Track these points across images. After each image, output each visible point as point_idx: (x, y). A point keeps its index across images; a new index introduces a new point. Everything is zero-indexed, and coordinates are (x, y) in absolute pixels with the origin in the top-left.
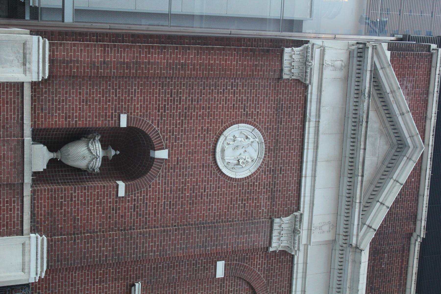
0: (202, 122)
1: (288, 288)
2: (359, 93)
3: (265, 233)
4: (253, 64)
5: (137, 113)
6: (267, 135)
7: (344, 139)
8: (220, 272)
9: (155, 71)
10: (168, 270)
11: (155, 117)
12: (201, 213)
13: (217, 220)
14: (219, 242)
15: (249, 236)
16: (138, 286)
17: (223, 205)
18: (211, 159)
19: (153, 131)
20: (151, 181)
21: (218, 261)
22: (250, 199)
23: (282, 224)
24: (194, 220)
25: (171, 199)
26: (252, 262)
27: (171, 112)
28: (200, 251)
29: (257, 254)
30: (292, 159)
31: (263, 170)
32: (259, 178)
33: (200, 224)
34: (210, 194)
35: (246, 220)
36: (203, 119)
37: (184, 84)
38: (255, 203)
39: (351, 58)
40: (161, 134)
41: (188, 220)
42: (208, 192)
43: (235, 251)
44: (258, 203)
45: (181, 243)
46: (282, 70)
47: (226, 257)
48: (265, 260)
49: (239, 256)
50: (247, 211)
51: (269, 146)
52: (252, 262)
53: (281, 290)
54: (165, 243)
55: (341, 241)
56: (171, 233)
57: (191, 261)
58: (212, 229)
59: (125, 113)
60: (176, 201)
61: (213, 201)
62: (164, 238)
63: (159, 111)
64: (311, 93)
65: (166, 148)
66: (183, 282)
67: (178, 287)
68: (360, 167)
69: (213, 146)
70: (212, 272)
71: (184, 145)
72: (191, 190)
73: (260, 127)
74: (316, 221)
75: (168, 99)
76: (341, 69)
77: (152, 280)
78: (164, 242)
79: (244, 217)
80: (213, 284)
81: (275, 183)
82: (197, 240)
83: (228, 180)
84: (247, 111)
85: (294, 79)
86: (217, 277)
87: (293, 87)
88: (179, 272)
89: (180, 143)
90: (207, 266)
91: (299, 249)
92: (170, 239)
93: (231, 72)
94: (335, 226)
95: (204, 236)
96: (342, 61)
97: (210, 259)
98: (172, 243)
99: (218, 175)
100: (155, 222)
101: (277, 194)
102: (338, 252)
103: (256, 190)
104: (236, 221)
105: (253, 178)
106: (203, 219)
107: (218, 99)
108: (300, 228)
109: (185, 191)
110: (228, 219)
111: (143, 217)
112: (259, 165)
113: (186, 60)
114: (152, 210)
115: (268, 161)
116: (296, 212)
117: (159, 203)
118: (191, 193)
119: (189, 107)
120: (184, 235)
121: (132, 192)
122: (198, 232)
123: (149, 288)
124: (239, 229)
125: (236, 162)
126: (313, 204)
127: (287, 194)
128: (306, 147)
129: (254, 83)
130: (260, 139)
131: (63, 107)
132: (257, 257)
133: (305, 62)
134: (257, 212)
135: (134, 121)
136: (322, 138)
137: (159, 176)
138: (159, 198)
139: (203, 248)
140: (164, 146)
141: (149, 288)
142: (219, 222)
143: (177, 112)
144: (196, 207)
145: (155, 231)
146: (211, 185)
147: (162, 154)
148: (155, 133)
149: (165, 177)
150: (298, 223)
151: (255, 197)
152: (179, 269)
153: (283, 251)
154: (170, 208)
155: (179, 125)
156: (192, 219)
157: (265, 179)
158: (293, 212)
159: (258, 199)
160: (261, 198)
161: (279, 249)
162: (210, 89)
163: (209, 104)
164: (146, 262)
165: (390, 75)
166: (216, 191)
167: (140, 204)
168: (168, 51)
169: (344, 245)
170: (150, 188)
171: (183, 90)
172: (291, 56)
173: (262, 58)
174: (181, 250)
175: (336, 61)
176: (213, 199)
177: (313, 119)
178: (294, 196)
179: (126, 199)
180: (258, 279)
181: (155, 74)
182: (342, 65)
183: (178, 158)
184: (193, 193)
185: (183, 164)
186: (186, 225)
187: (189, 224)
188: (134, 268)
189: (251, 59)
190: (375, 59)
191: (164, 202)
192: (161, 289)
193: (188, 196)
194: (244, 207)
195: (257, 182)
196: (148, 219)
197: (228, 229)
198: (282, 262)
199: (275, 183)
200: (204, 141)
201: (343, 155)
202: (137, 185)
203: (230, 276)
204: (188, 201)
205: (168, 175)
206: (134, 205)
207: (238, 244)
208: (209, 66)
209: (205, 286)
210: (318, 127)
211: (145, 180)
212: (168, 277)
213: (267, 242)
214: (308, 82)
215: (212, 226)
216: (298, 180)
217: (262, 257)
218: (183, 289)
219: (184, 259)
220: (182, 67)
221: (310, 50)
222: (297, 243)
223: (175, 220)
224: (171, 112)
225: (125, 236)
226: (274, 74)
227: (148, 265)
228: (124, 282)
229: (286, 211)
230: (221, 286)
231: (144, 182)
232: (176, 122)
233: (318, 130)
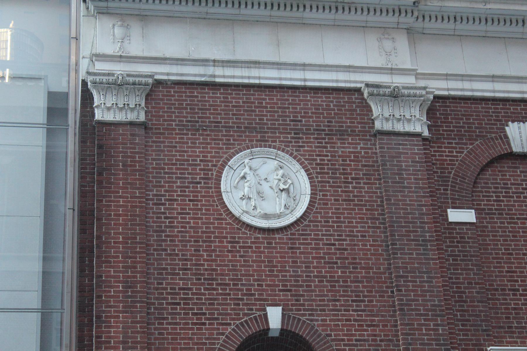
0: (220, 251)
1: (488, 104)
3: (400, 144)
4: (122, 170)
6: (238, 145)
7: (241, 18)
8: (467, 216)
9: (138, 332)
10: (465, 302)
11: (214, 329)
12: (370, 250)
13: (380, 223)
14: (416, 218)
15: (406, 170)
18: (280, 236)
19: (237, 333)
20: (320, 334)
21: (448, 219)
22: (343, 169)
23: (384, 117)
24: (382, 261)
25: (348, 301)
26: (448, 164)
27: (204, 304)
28: (431, 250)
29: (435, 156)
30: (277, 104)
31: (296, 151)
32: (309, 155)
33: (387, 251)
34: (338, 235)
35: (379, 175)
36: (214, 251)
37: (158, 284)
38: (350, 161)
39: (109, 11)
41: (382, 270)
42: (335, 240)
43: (431, 192)
44: (350, 157)
45: (420, 282)
46: (132, 124)
47: (440, 207)
48: (444, 143)
49: (439, 185)
50: (364, 174)
51: (257, 141)
52: (448, 164)
53: (492, 116)
54: (422, 308)
55: (409, 20)
56: (404, 298)
57: (450, 265)
58: (394, 231)
60: (352, 291)
61: (350, 231)
62: (412, 310)
63: (204, 324)
64: (168, 74)
65: (265, 310)
66: (484, 276)
67: (493, 285)
69: (259, 233)
71: (258, 280)
72: (333, 268)
73: (225, 156)
74: (378, 61)
75: (184, 309)
76: (128, 27)
77: (484, 328)
78: (420, 310)
79: (375, 179)
80: (487, 227)
81: (317, 130)
82: (415, 256)
83: (314, 206)
84: (200, 178)
85: (146, 103)
86: (475, 221)
87: (159, 104)
88: (469, 283)
89: (256, 287)
90: (457, 238)
91: (425, 88)
92: (413, 300)
93: (136, 207)
94: (384, 30)
95: (407, 245)
96: (114, 25)
97: (445, 233)
98: (422, 296)
99: (306, 223)
100: (387, 326)
101: (335, 126)
102: (427, 24)
103: (328, 160)
104: (381, 193)
105: (309, 167)
107: (182, 227)
108: (389, 87)
109: (334, 277)
110: (377, 206)
112: (287, 156)
113: (119, 282)
114: (367, 330)
115: (280, 142)
116: (362, 94)
117: (355, 320)
118: (338, 268)
119: (195, 274)
120: (407, 277)
122: (401, 254)
123: (497, 332)
124: (393, 187)
125: (284, 195)
126: (349, 67)
127: (334, 110)
128: (257, 81)
129: (153, 168)
130: (245, 157)
132: (439, 156)
133: (117, 85)
134: (366, 158)
137: (312, 320)
138: (347, 320)
139: (427, 246)
140: (262, 313)
141: (497, 332)
142: (384, 219)
143: (204, 294)
144: (360, 259)
145: (401, 324)
146: (323, 235)
147: (275, 317)
148: (240, 329)
149: (312, 310)
150: (382, 91)
151: (341, 162)
152: (463, 283)
153: (428, 114)
154: (364, 301)
155: (226, 289)
156: (381, 264)
157: (311, 147)
158: (363, 99)
159: (344, 157)
160: (342, 152)
161: (425, 120)
163: (190, 241)
164: (454, 338)
166: (333, 227)
168: (104, 312)
169: (416, 14)
170: (330, 335)
171: (167, 284)
172: (109, 109)
174: (432, 282)
175: (114, 35)
176: (345, 231)
177: (211, 70)
178: (338, 98)
180: (475, 153)
181: (143, 332)
182: (122, 26)
183: (280, 291)
184: (336, 263)
185: (290, 281)
186: (391, 274)
187: (389, 269)
189: (114, 174)
191: (353, 311)
192: (498, 313)
193: (342, 272)
194: (358, 179)
195: (316, 160)
196: (383, 337)
197: (394, 204)
198: (446, 114)
199: (317, 130)
200: (251, 247)
201: (268, 20)
203: (473, 200)
204: (350, 272)
205: (308, 305)
207: (420, 188)
208: (127, 243)
209: (490, 240)
210: (223, 62)
212: (478, 302)
214: (150, 81)
215: (391, 231)
216: (310, 93)
217: (438, 147)
219: (446, 276)
220: (130, 287)
221: (98, 78)
222: (415, 91)
223: (383, 292)
224: (204, 304)
226: (138, 135)
227: (460, 335)
229: (362, 111)
230: (488, 214)
232: (221, 294)
233: (229, 62)
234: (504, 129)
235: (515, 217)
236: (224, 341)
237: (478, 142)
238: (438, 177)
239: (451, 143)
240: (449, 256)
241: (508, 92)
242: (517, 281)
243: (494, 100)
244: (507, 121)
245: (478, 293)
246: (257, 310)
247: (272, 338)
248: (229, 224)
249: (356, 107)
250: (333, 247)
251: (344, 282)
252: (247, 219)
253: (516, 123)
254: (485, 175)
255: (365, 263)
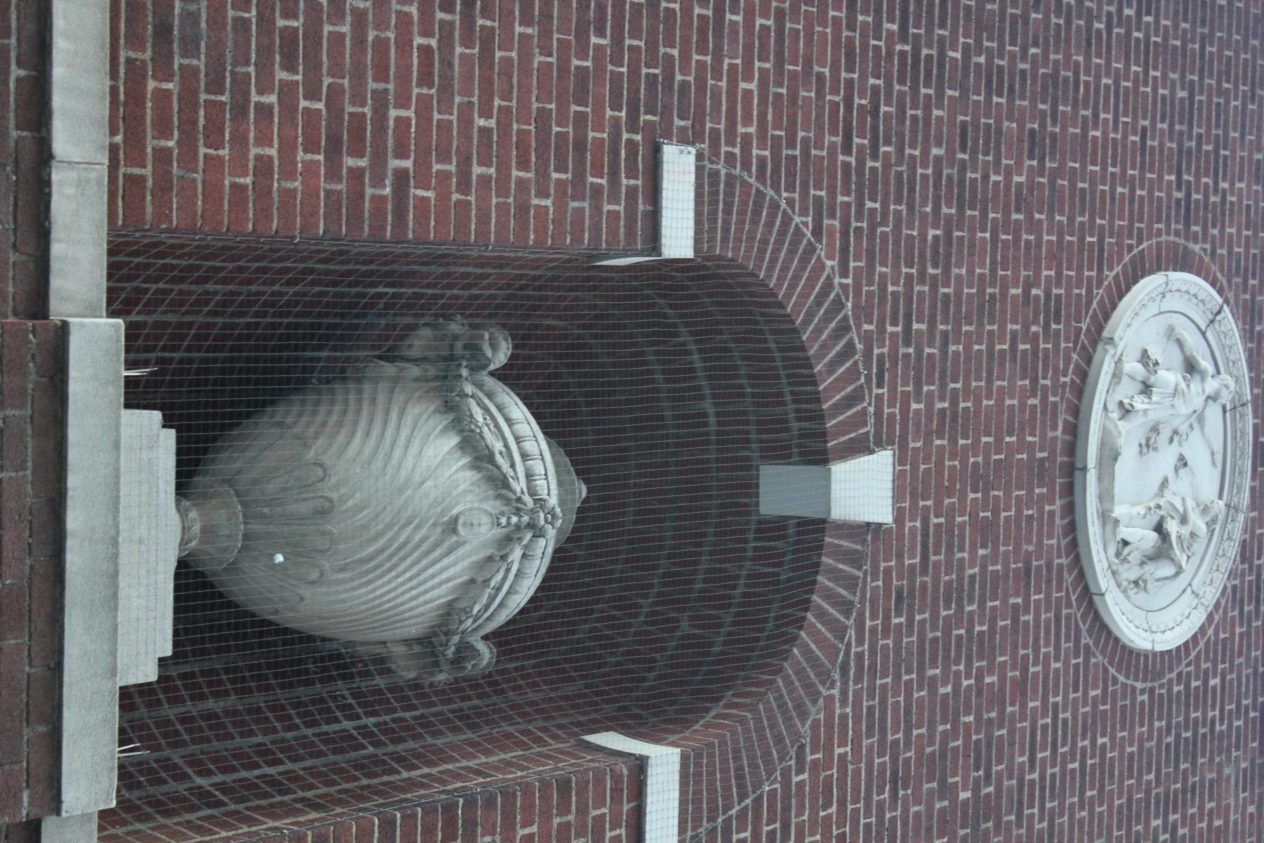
19: (818, 304)
59: (683, 141)
65: (880, 444)
99: (1086, 640)
131: (313, 35)
147: (862, 489)
202: (737, 752)
247: (750, 488)
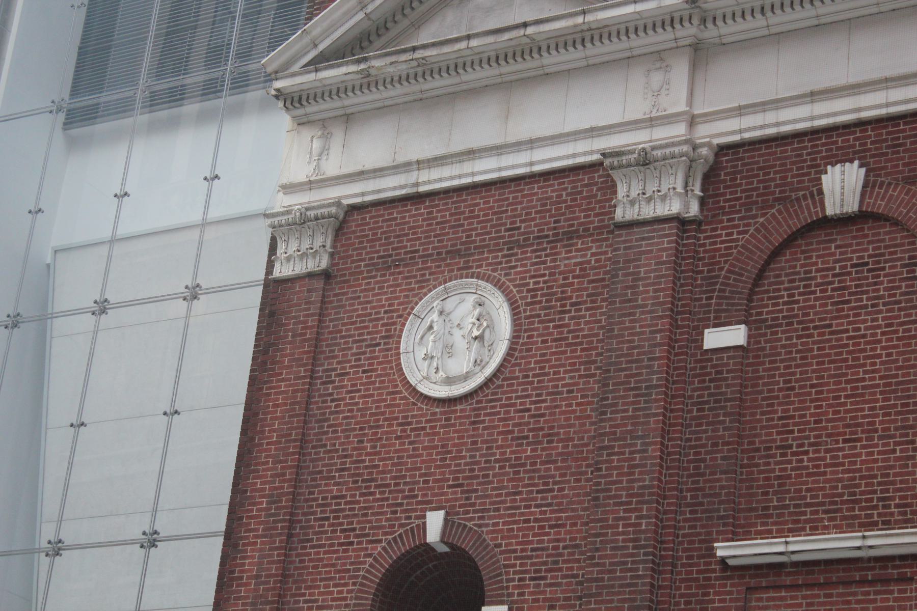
1: (803, 141)
2: (369, 82)
5: (349, 592)
7: (465, 87)
8: (733, 336)
10: (703, 475)
12: (574, 411)
16: (723, 549)
17: (567, 358)
18: (462, 407)
20: (488, 545)
40: (396, 532)
41: (586, 441)
45: (608, 455)
46: (310, 275)
48: (722, 221)
51: (459, 269)
54: (624, 493)
55: (688, 32)
64: (363, 194)
65: (424, 517)
68: (507, 36)
69: (437, 407)
70: (729, 358)
74: (638, 109)
78: (621, 496)
89: (421, 485)
94: (659, 58)
96: (312, 137)
99: (499, 382)
100: (575, 524)
106: (589, 403)
108: (631, 152)
111: (561, 555)
112: (489, 286)
117: (536, 520)
118: (528, 444)
120: (613, 447)
121: (502, 588)
125: (476, 344)
126: (592, 129)
130: (434, 299)
132: (711, 244)
133: (302, 222)
135: (362, 598)
136: (457, 146)
137: (480, 526)
138: (526, 521)
149: (483, 511)
150: (624, 159)
151: (561, 282)
160: (565, 265)
162: (327, 433)
165: (325, 25)
167: (532, 564)
168: (242, 538)
173: (283, 325)
177: (412, 177)
179: (516, 602)
184: (527, 437)
188: (683, 565)
190: (296, 68)
197: (617, 336)
201: (499, 80)
206: (531, 579)
210: (428, 161)
211: (482, 558)
213: (664, 229)
218: (762, 428)
220: (274, 502)
221: (276, 220)
222: (672, 149)
225: (591, 595)
228: (713, 586)
231: (487, 561)
233: (436, 159)
234: (820, 179)
235: (811, 325)
236: (371, 565)
237: (774, 211)
238: (702, 279)
239: (733, 220)
240: (693, 404)
241: (835, 114)
242: (792, 432)
243: (814, 133)
244: (826, 165)
245: (723, 458)
246: (417, 518)
248: (405, 398)
249: (598, 190)
250: (527, 414)
251: (532, 464)
252: (427, 389)
253: (839, 165)
254: (780, 262)
255: (565, 433)
